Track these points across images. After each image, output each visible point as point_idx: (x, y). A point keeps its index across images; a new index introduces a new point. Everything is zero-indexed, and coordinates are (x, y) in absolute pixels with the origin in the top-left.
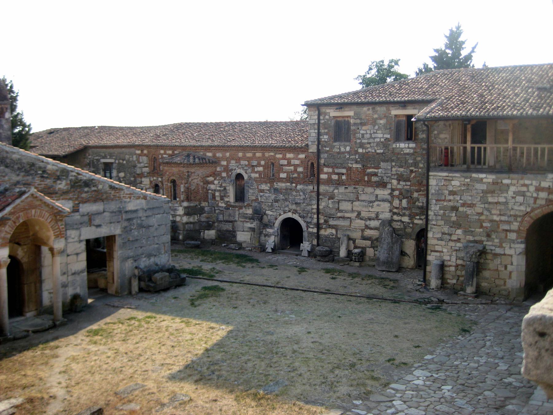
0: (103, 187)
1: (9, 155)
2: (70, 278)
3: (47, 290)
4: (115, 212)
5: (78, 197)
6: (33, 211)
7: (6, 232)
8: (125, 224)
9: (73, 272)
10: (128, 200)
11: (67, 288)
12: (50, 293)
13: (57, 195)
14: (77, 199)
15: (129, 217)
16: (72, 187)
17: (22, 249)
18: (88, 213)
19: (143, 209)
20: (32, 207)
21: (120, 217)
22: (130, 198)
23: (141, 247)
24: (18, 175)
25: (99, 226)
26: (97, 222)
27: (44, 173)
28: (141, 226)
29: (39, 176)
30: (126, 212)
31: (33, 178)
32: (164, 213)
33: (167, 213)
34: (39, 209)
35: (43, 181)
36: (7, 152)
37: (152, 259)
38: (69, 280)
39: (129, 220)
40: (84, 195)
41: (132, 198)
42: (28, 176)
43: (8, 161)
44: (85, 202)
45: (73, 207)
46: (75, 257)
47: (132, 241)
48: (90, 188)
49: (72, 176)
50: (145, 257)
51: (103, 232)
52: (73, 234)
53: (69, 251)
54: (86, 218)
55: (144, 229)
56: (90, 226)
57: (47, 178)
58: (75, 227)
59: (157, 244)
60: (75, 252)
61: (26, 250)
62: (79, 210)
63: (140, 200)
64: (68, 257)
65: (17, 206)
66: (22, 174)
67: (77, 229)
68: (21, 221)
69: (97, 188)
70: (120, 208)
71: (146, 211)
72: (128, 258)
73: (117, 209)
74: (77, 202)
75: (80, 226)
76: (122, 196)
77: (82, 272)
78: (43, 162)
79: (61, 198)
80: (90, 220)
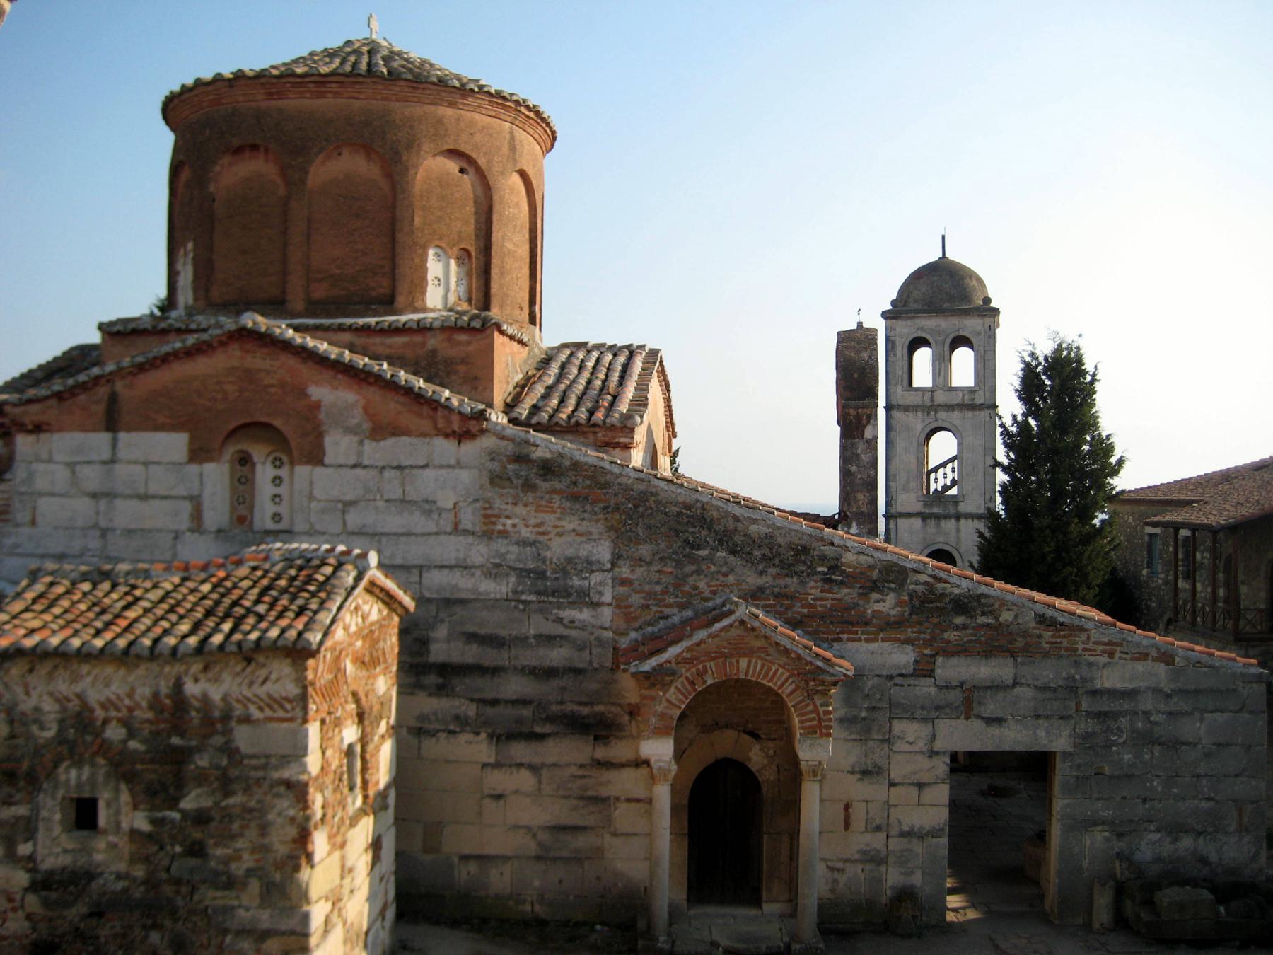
0: (1016, 617)
1: (740, 526)
2: (895, 844)
3: (822, 859)
4: (1055, 690)
5: (933, 639)
6: (743, 663)
7: (668, 701)
9: (906, 828)
10: (1104, 659)
11: (883, 868)
12: (832, 869)
13: (870, 629)
14: (928, 643)
15: (1106, 709)
17: (761, 749)
18: (962, 684)
19: (1157, 691)
20: (741, 650)
22: (1111, 655)
23: (1145, 800)
24: (761, 573)
26: (991, 707)
28: (1147, 739)
29: (818, 577)
30: (1094, 693)
31: (802, 583)
32: (1240, 710)
33: (1251, 712)
34: (759, 657)
35: (829, 591)
36: (736, 519)
37: (1186, 843)
38: (890, 848)
39: (1101, 716)
40: (951, 635)
41: (1117, 655)
42: (787, 575)
43: (738, 539)
44: (954, 654)
45: (916, 662)
46: (914, 791)
47: (1111, 777)
48: (972, 617)
50: (1158, 830)
51: (1013, 737)
52: (911, 732)
53: (896, 774)
54: (955, 696)
55: (1157, 750)
56: (967, 718)
57: (842, 583)
58: (918, 714)
59: (1209, 799)
60: (915, 779)
61: (771, 752)
62: (933, 671)
63: (1149, 662)
64: (892, 789)
65: (698, 645)
66: (773, 571)
67: (924, 720)
68: (710, 682)
69: (997, 619)
71: (1168, 696)
72: (1095, 824)
73: (1061, 683)
74: (927, 652)
75: (934, 714)
76: (1080, 647)
77: (934, 833)
78: (832, 544)
80: (968, 701)
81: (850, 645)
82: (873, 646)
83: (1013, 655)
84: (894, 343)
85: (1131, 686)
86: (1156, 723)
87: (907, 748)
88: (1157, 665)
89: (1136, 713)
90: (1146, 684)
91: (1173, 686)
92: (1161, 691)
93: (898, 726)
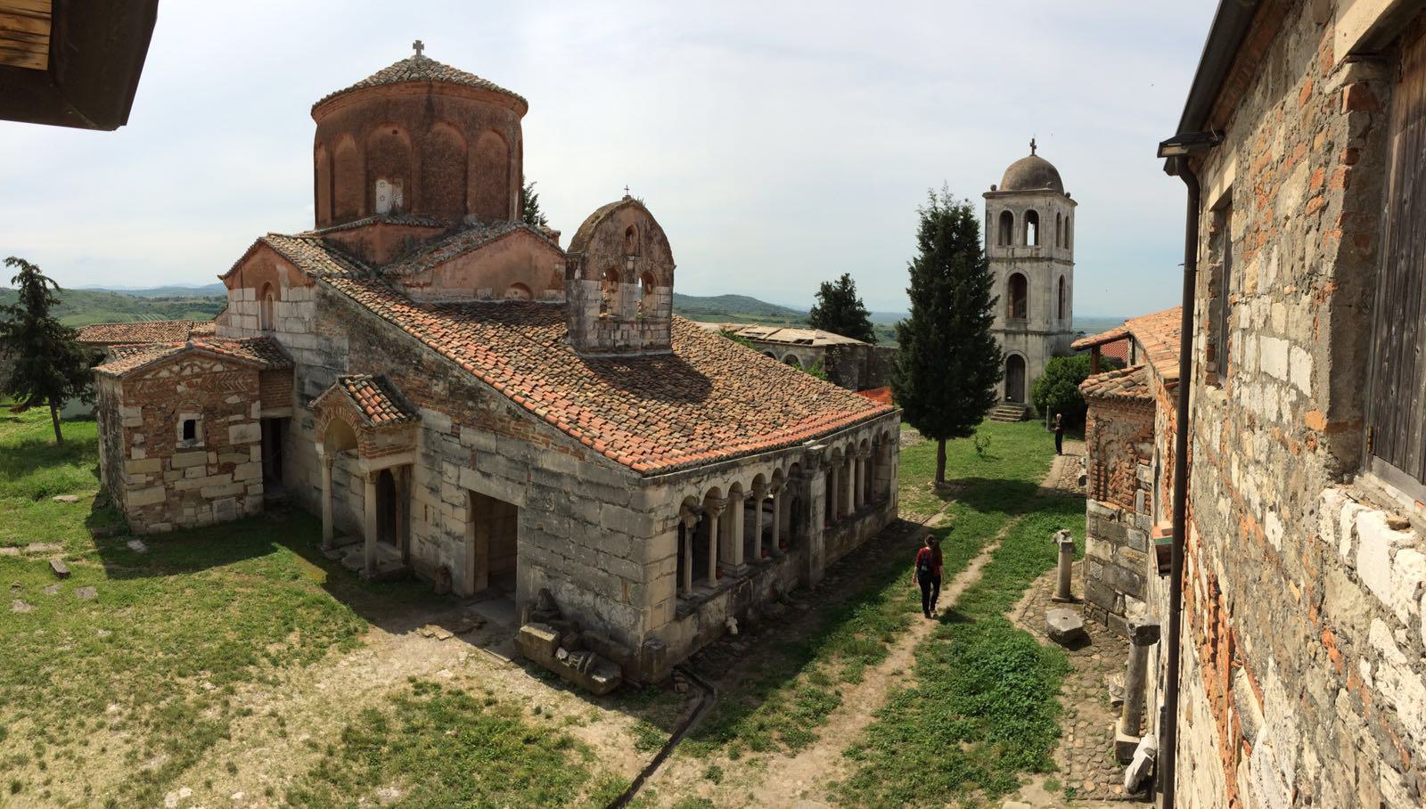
8: (533, 493)
10: (543, 447)
15: (544, 483)
16: (452, 393)
18: (472, 445)
19: (573, 478)
21: (526, 475)
22: (548, 446)
25: (487, 475)
26: (485, 466)
27: (419, 367)
28: (566, 512)
30: (539, 470)
32: (626, 506)
41: (551, 445)
45: (452, 427)
47: (546, 533)
49: (453, 376)
51: (494, 488)
52: (450, 469)
54: (467, 453)
55: (572, 522)
57: (422, 371)
58: (454, 460)
66: (397, 360)
67: (455, 465)
70: (525, 456)
71: (580, 483)
75: (460, 462)
79: (438, 407)
80: (474, 457)
81: (426, 410)
82: (435, 413)
83: (495, 432)
84: (991, 215)
85: (559, 471)
86: (573, 502)
87: (449, 481)
88: (573, 458)
89: (560, 492)
90: (567, 472)
91: (583, 477)
92: (576, 478)
93: (445, 466)
